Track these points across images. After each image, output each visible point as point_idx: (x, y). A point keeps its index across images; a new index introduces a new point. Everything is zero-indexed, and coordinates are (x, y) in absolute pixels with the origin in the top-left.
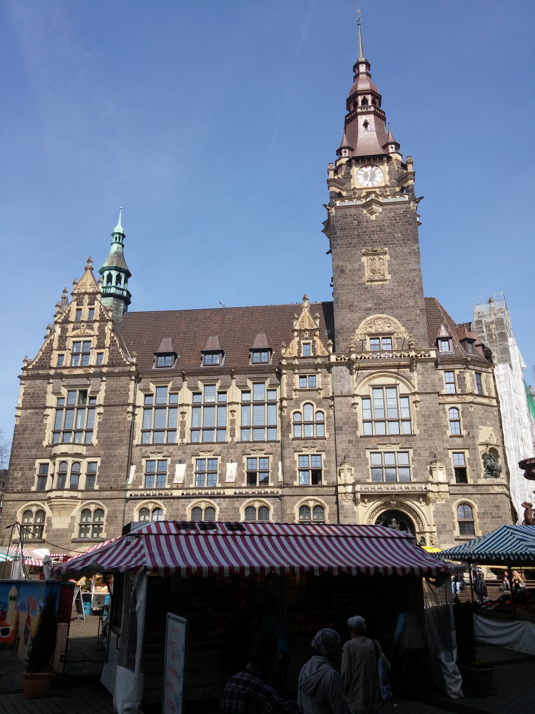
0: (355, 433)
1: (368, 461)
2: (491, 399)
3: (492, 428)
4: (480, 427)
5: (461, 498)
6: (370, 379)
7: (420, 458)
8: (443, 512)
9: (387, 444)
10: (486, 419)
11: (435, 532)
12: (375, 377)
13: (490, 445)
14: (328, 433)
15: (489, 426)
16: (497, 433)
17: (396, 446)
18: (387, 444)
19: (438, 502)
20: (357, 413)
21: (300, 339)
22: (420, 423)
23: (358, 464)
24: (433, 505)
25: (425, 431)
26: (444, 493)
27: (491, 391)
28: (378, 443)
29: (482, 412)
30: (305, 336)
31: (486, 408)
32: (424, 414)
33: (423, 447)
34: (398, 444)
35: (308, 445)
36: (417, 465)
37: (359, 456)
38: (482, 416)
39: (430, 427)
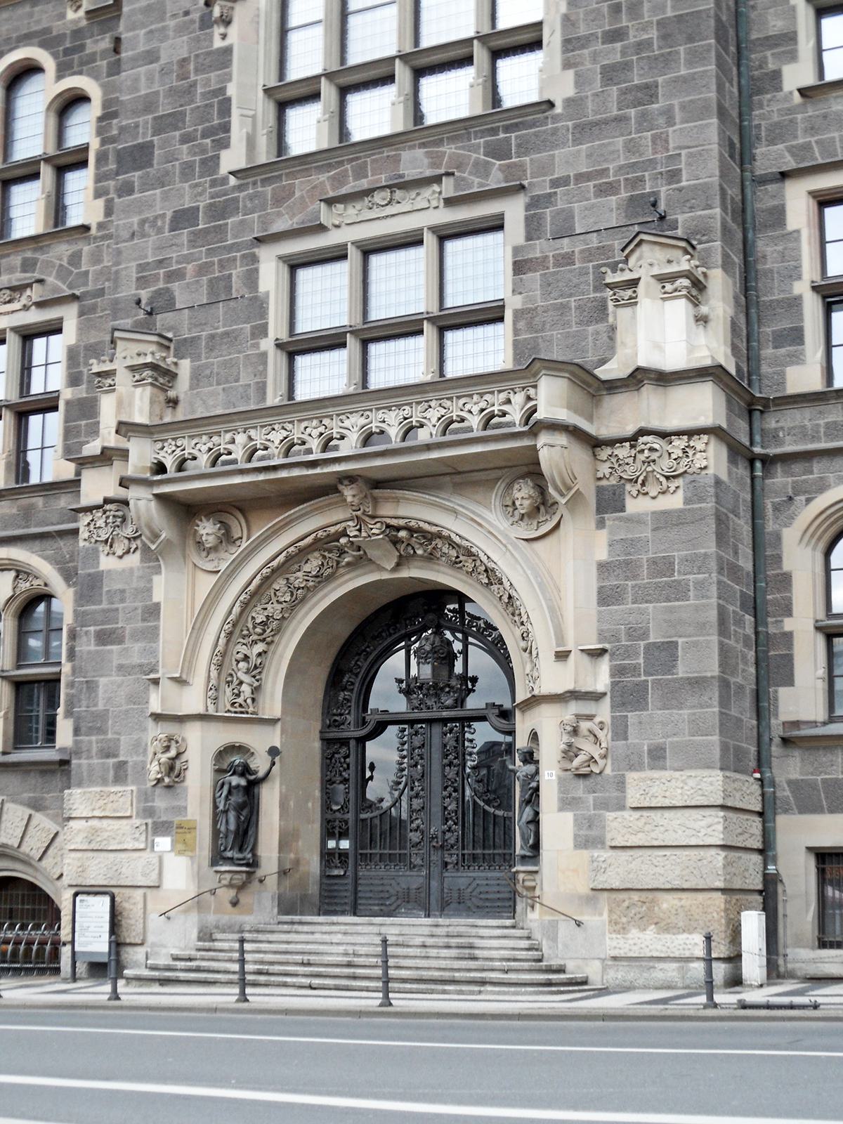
0: (211, 164)
1: (263, 312)
7: (565, 245)
8: (663, 566)
11: (596, 697)
14: (100, 203)
17: (427, 192)
22: (583, 31)
23: (212, 337)
24: (601, 524)
25: (611, 74)
28: (331, 194)
33: (581, 177)
34: (437, 179)
36: (546, 295)
37: (220, 291)
39: (641, 46)
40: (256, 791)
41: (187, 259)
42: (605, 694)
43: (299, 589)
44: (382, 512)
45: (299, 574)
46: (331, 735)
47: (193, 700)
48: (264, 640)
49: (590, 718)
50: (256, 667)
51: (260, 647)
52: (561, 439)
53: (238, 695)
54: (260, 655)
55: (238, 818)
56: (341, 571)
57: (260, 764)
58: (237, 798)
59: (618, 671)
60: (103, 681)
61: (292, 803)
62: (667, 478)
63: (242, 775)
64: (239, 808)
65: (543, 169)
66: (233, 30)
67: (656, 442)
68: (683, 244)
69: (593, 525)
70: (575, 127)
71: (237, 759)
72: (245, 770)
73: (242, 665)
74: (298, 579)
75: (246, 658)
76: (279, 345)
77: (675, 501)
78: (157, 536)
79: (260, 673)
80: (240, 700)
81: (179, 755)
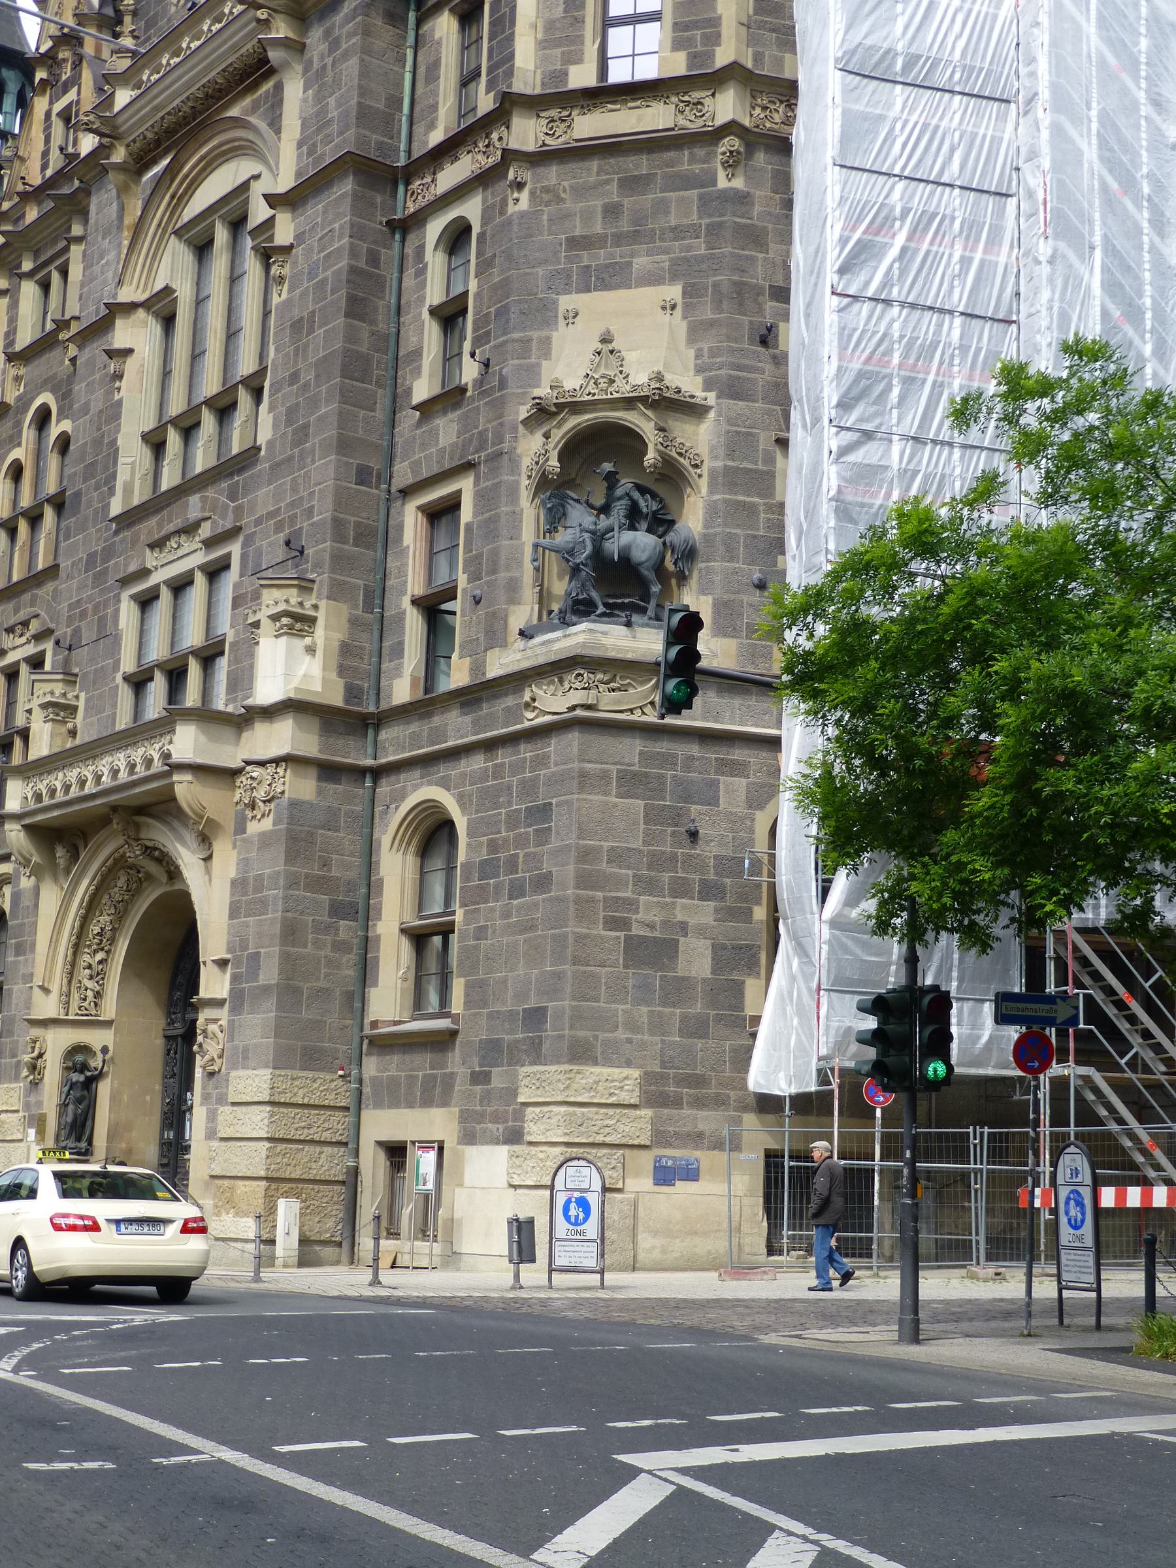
2: (696, 95)
3: (674, 292)
4: (566, 302)
5: (416, 787)
6: (180, 201)
9: (168, 537)
10: (635, 237)
12: (194, 184)
13: (576, 407)
15: (652, 279)
16: (709, 314)
18: (168, 537)
19: (253, 828)
20: (120, 402)
21: (51, 103)
23: (96, 670)
26: (271, 769)
27: (714, 39)
29: (598, 204)
30: (64, 78)
31: (641, 164)
32: (296, 313)
35: (22, 615)
38: (598, 228)
40: (94, 1085)
41: (90, 599)
42: (225, 1000)
43: (119, 902)
44: (142, 836)
45: (116, 889)
46: (168, 1033)
47: (48, 1007)
48: (102, 949)
49: (215, 1021)
50: (98, 974)
51: (100, 956)
52: (188, 777)
53: (85, 999)
54: (100, 962)
55: (76, 1110)
56: (145, 884)
57: (96, 1063)
58: (76, 1093)
59: (235, 979)
60: (15, 988)
61: (125, 1097)
62: (264, 802)
63: (81, 1072)
64: (79, 1101)
65: (253, 505)
66: (124, 385)
67: (256, 772)
68: (295, 582)
69: (230, 846)
70: (271, 468)
71: (79, 1058)
72: (84, 1067)
73: (87, 971)
74: (116, 893)
75: (90, 967)
76: (126, 679)
77: (267, 824)
78: (29, 861)
79: (103, 979)
80: (85, 1004)
81: (40, 1056)
